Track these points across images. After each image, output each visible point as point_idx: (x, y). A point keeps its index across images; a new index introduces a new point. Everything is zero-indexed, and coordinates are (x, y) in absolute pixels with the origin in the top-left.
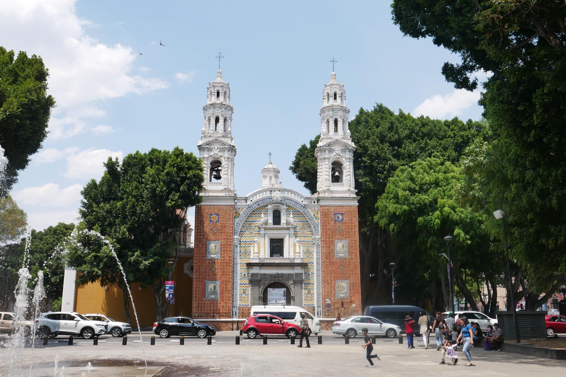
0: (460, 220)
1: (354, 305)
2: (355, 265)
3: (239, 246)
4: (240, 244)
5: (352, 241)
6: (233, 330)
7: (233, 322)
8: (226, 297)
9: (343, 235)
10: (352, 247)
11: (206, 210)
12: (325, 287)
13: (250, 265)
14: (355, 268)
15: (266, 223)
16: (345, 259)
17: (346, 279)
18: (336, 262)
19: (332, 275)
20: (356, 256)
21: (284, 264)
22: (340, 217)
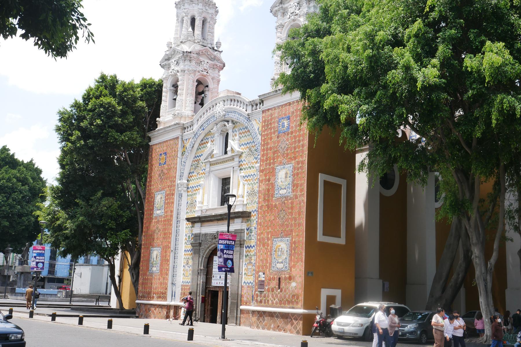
1: (294, 284)
2: (300, 208)
3: (185, 194)
4: (188, 192)
5: (298, 164)
6: (168, 317)
7: (168, 307)
9: (287, 155)
10: (298, 174)
11: (157, 150)
12: (259, 251)
13: (193, 221)
14: (299, 214)
15: (211, 155)
16: (286, 198)
17: (286, 236)
18: (276, 205)
19: (270, 230)
20: (302, 190)
22: (286, 123)
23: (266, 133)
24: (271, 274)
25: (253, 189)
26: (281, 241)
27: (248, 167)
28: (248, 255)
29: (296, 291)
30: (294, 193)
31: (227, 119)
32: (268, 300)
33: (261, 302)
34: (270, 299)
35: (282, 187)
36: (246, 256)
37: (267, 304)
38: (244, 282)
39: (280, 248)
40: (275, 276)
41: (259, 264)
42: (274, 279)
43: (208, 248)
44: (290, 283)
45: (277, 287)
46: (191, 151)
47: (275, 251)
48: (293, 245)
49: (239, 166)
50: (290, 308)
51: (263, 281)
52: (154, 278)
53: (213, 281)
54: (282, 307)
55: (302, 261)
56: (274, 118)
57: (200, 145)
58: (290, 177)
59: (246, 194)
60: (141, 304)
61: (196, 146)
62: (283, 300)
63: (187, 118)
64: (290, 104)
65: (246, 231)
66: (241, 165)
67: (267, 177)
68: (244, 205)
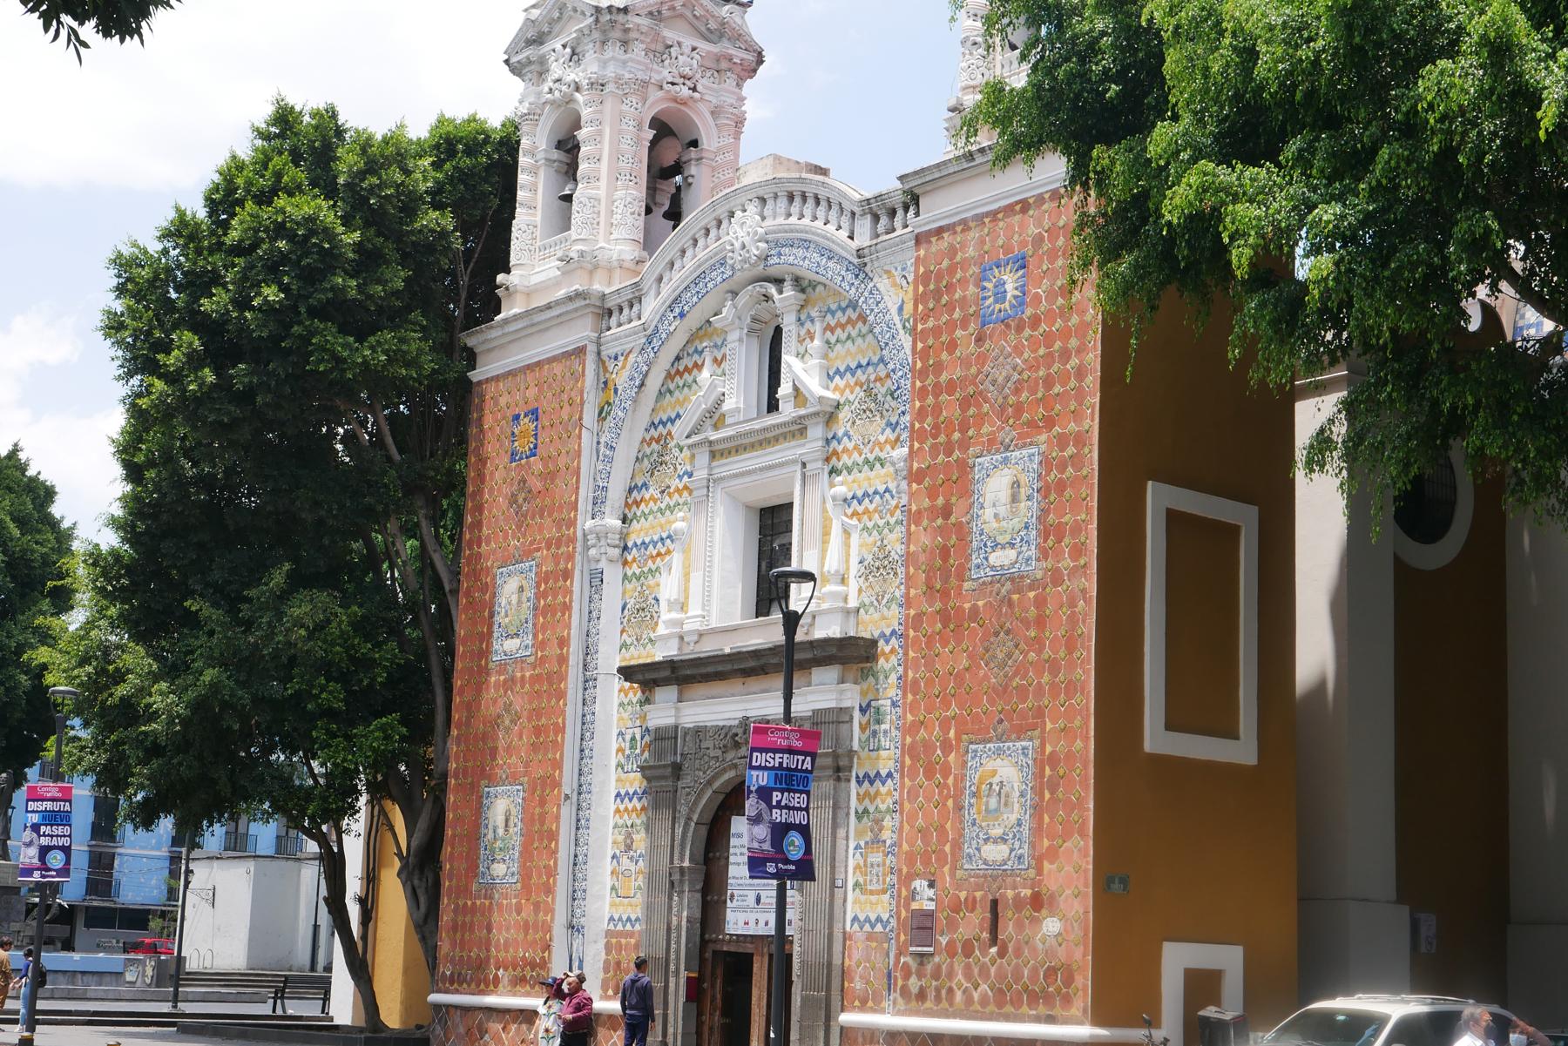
0: (1458, 52)
1: (1051, 926)
2: (1073, 620)
3: (613, 575)
4: (625, 563)
5: (1062, 442)
8: (540, 876)
9: (1019, 409)
10: (1061, 486)
11: (503, 401)
12: (913, 796)
14: (1070, 649)
15: (715, 416)
16: (1017, 581)
17: (1020, 732)
19: (954, 709)
20: (1077, 551)
21: (737, 656)
23: (930, 324)
24: (959, 888)
25: (882, 547)
26: (999, 753)
27: (860, 460)
28: (866, 811)
29: (1061, 953)
30: (1049, 564)
31: (772, 271)
32: (950, 990)
33: (921, 995)
34: (960, 986)
35: (1000, 539)
36: (859, 817)
37: (945, 1004)
38: (855, 919)
39: (996, 780)
40: (978, 894)
41: (911, 844)
42: (971, 905)
43: (709, 783)
44: (1036, 922)
45: (985, 935)
46: (635, 401)
47: (974, 795)
48: (1048, 771)
49: (827, 460)
50: (1038, 1019)
51: (929, 915)
52: (500, 906)
53: (730, 916)
54: (1007, 1018)
55: (1083, 835)
56: (965, 264)
57: (669, 376)
58: (1029, 498)
59: (854, 568)
60: (449, 1007)
61: (654, 382)
62: (1010, 988)
63: (617, 273)
64: (1025, 206)
65: (857, 714)
66: (835, 453)
67: (940, 501)
68: (847, 612)
